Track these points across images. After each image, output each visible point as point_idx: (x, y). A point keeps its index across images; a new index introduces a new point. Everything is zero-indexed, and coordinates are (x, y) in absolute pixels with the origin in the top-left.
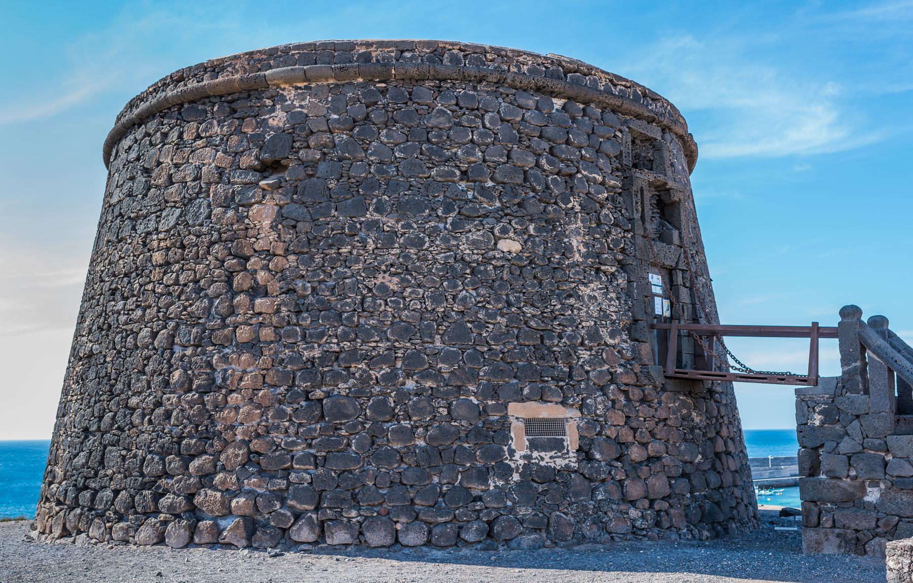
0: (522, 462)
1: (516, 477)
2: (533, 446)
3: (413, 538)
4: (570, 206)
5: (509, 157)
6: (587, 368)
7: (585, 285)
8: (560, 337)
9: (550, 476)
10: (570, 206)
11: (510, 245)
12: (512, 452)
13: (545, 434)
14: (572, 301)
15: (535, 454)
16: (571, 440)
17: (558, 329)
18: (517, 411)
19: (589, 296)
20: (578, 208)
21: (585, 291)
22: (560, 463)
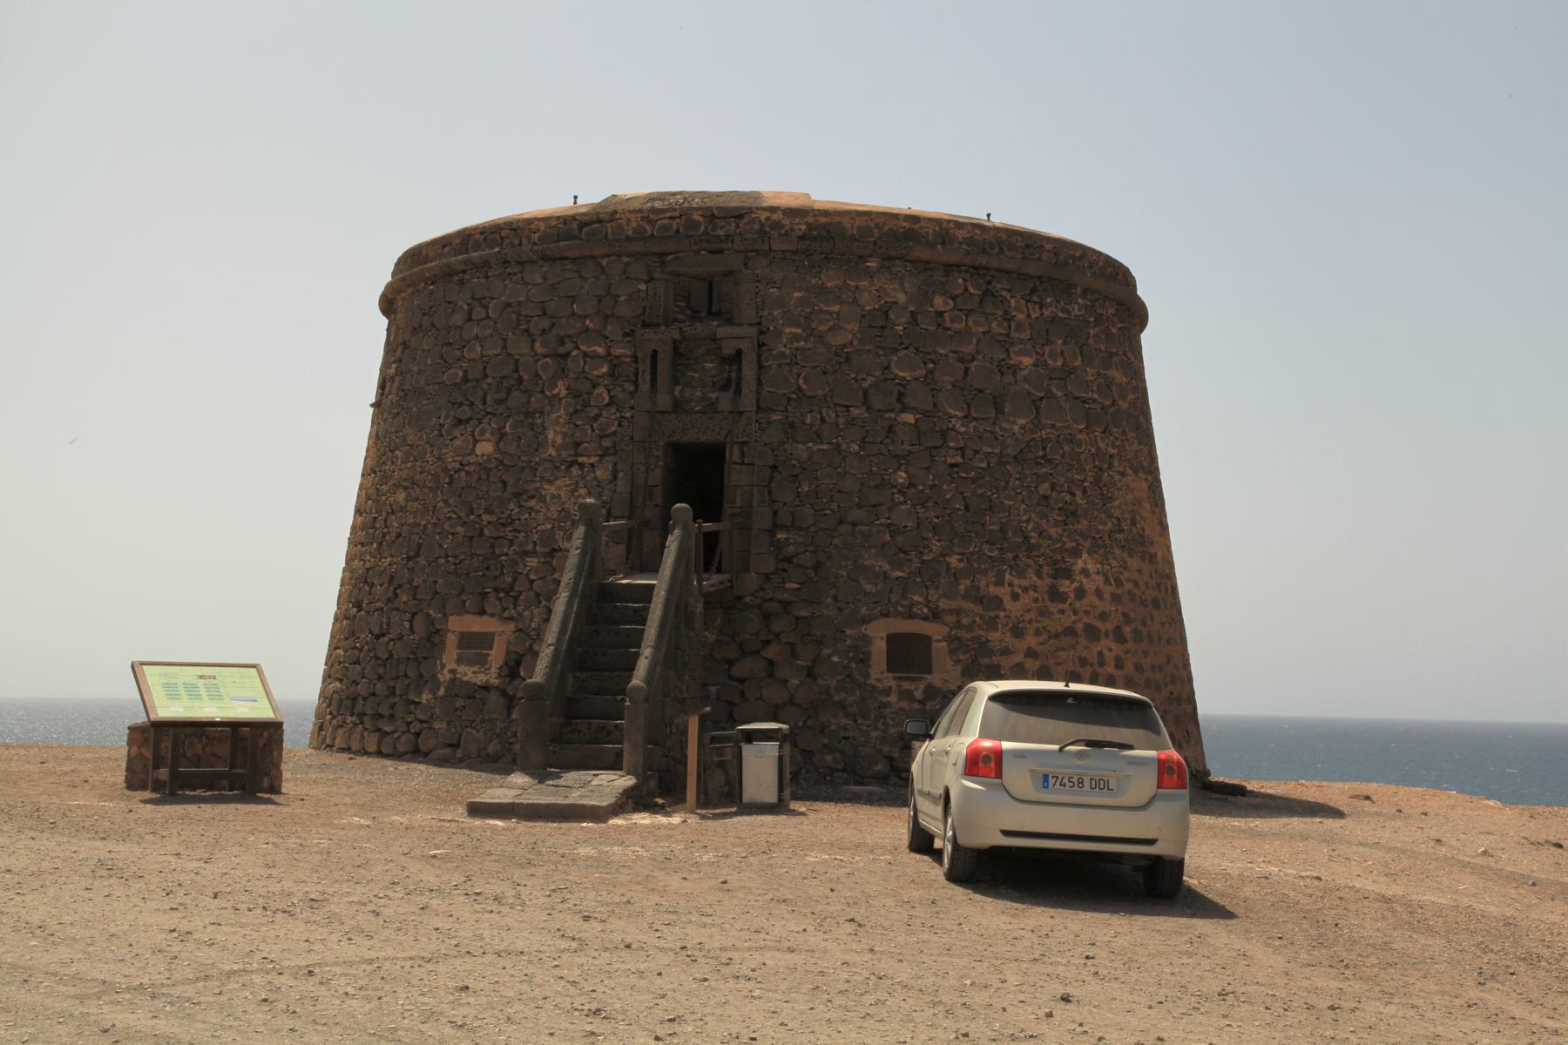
0: (448, 676)
1: (442, 692)
2: (460, 661)
3: (372, 748)
4: (556, 392)
5: (504, 347)
6: (533, 577)
7: (550, 482)
8: (511, 543)
9: (476, 694)
10: (556, 392)
11: (485, 448)
12: (443, 666)
13: (475, 645)
14: (532, 503)
15: (462, 669)
16: (496, 657)
17: (510, 536)
18: (458, 624)
19: (553, 497)
20: (564, 392)
21: (550, 489)
22: (480, 679)
